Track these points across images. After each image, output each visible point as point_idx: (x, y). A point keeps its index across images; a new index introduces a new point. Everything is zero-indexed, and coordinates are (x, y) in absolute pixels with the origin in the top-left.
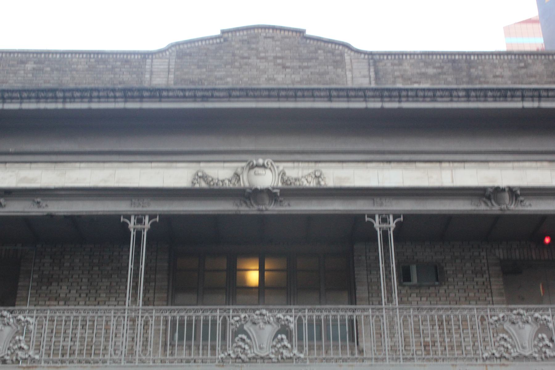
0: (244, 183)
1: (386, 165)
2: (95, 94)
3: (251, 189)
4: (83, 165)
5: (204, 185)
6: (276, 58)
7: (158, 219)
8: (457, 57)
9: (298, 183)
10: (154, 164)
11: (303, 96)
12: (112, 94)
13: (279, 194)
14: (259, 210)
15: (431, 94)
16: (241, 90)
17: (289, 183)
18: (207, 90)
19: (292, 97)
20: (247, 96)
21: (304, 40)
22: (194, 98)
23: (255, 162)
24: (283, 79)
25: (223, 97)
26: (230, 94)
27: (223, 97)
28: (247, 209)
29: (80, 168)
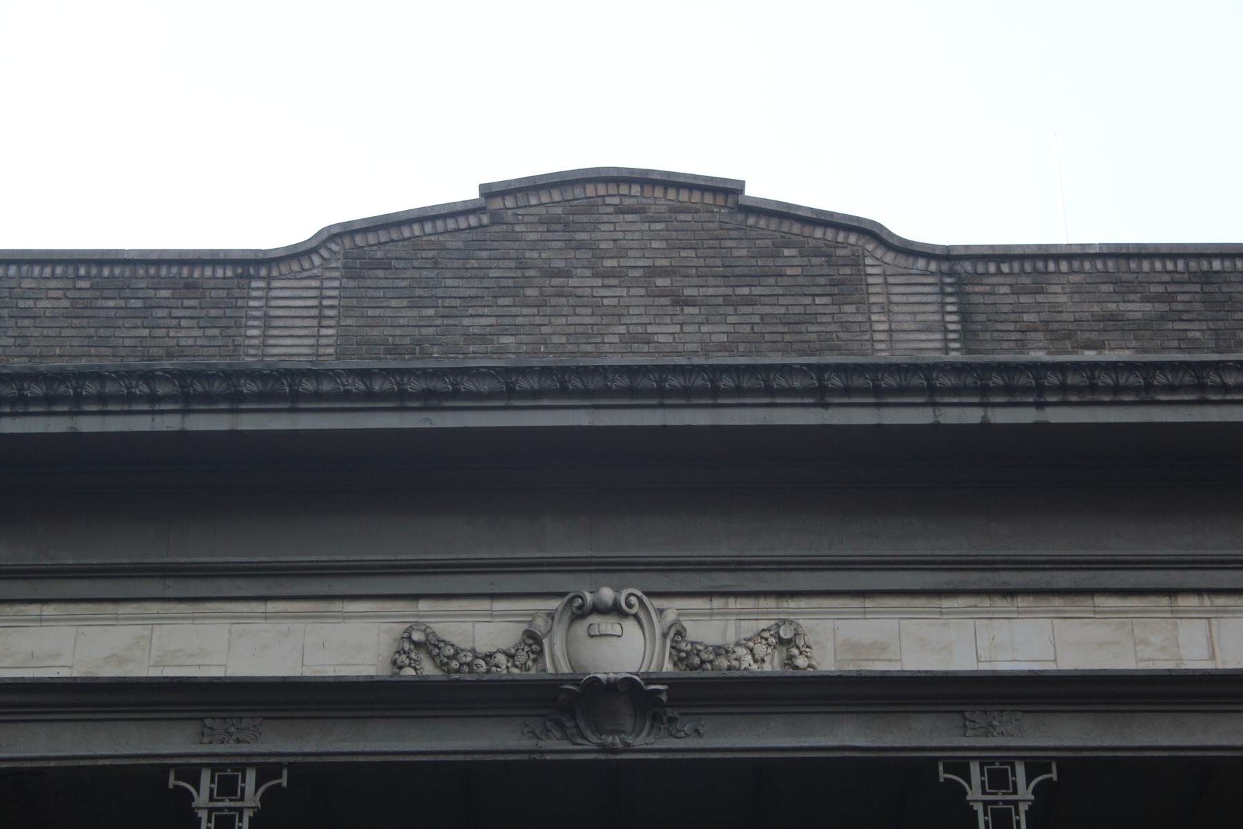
0: (556, 661)
1: (1000, 603)
2: (92, 388)
3: (575, 682)
4: (49, 610)
5: (429, 669)
6: (653, 272)
7: (284, 781)
8: (1217, 265)
9: (723, 662)
10: (272, 607)
11: (739, 391)
12: (143, 389)
13: (664, 698)
14: (604, 749)
15: (1135, 380)
16: (545, 371)
17: (697, 661)
18: (438, 373)
19: (701, 392)
20: (564, 392)
21: (740, 217)
22: (400, 400)
23: (589, 597)
24: (676, 338)
25: (491, 395)
26: (510, 384)
27: (491, 395)
28: (565, 745)
29: (40, 619)
